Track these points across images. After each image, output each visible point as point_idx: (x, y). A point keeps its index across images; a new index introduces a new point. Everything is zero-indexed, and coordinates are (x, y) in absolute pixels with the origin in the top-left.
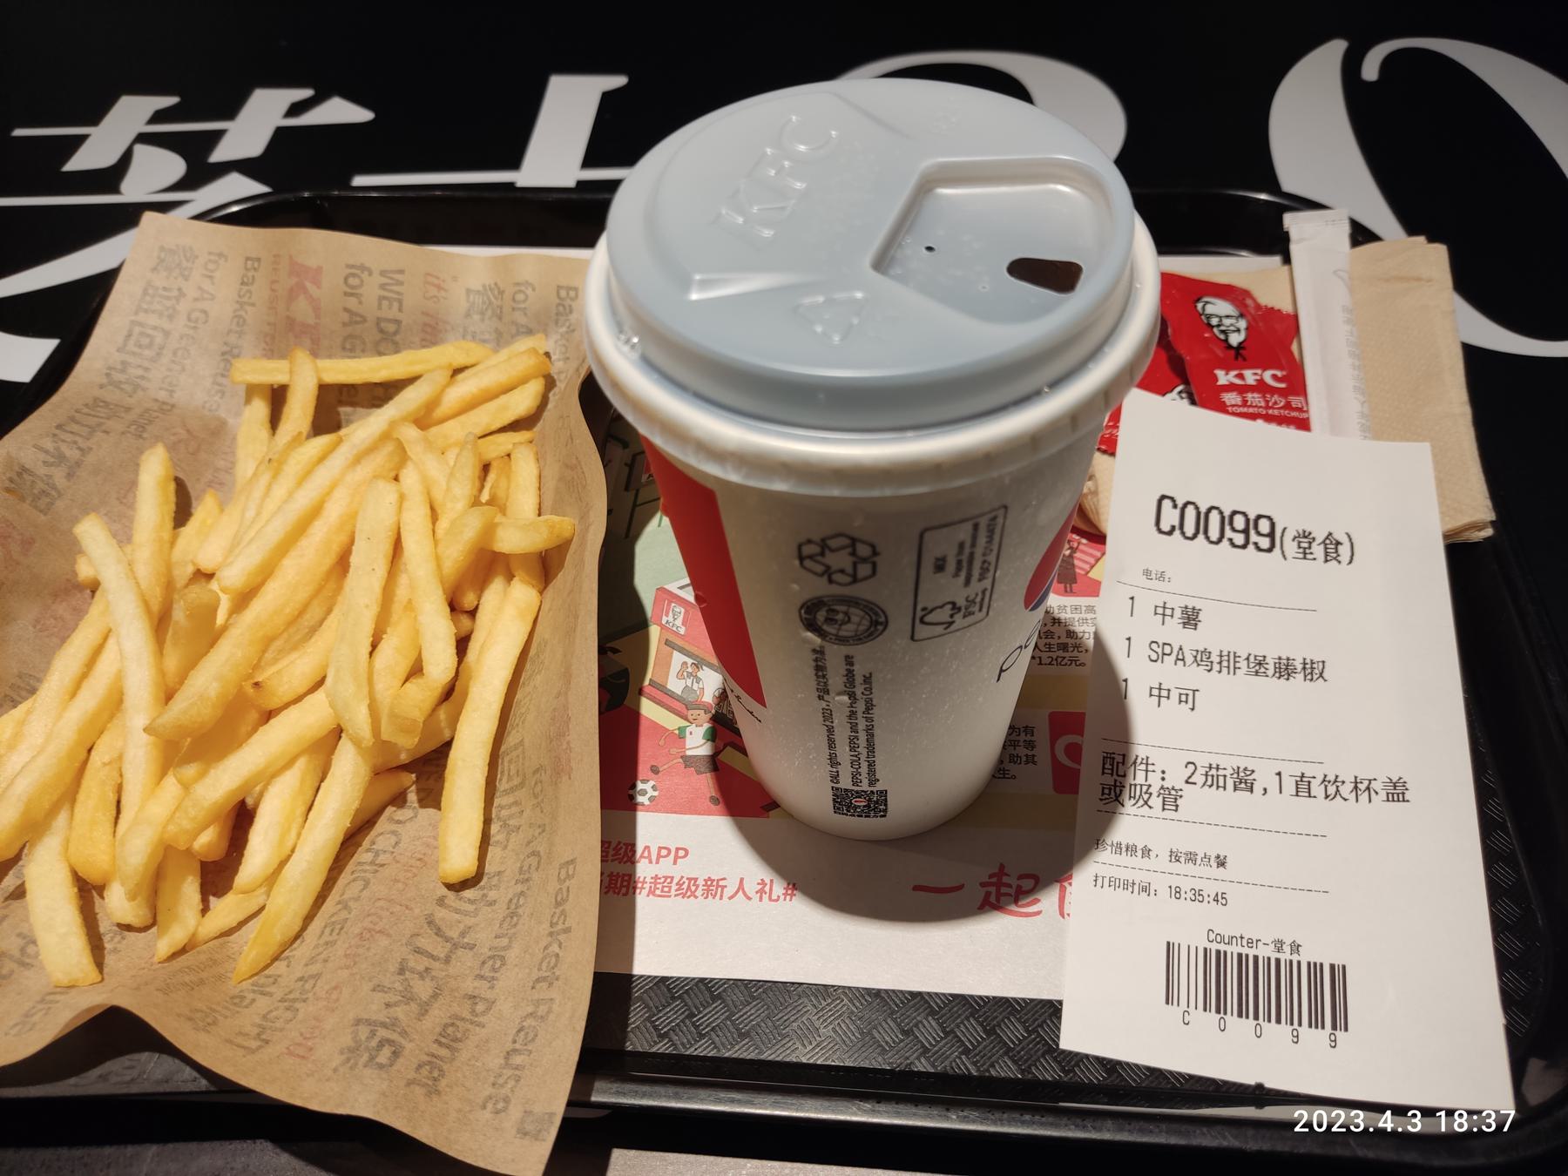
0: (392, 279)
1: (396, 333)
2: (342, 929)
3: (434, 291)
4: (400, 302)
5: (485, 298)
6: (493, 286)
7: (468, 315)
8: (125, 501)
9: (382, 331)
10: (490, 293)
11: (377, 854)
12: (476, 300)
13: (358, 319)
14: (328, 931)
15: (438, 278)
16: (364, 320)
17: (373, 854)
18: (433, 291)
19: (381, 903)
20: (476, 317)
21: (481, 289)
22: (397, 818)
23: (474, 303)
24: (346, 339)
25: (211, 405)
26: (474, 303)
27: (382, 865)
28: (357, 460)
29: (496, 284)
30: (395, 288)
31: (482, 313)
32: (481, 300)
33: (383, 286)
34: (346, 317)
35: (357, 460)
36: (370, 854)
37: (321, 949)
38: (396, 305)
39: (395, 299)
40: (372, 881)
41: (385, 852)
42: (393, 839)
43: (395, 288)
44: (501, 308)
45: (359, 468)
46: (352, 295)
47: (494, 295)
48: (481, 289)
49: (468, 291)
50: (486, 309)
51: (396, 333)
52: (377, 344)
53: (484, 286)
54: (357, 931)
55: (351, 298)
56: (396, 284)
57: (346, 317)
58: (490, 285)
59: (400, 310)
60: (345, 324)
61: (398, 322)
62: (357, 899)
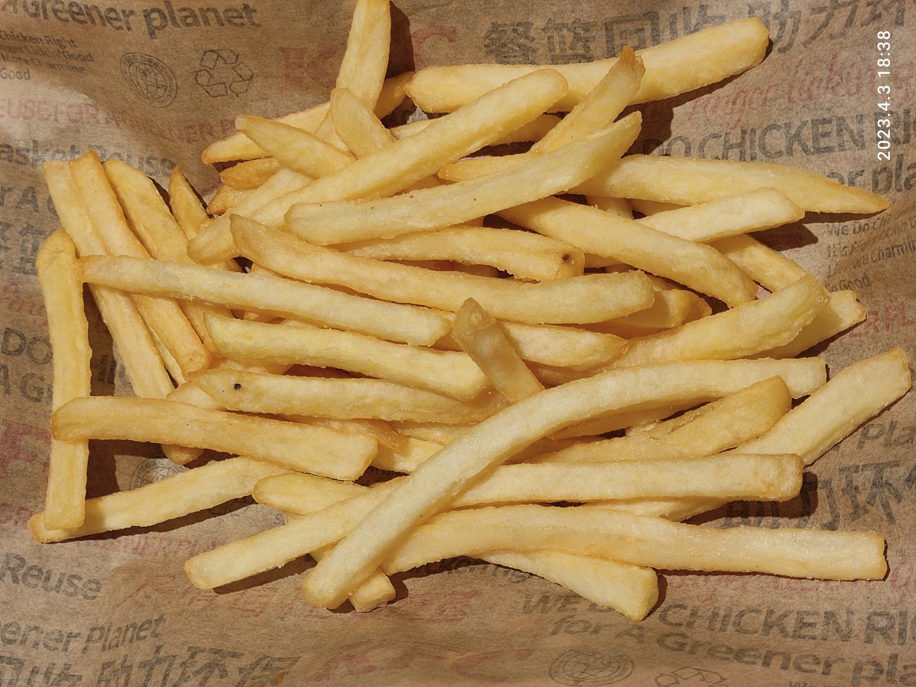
2: (825, 121)
14: (823, 143)
19: (795, 94)
25: (91, 589)
27: (744, 132)
37: (846, 136)
40: (765, 125)
41: (725, 142)
42: (711, 142)
54: (829, 96)
62: (788, 126)
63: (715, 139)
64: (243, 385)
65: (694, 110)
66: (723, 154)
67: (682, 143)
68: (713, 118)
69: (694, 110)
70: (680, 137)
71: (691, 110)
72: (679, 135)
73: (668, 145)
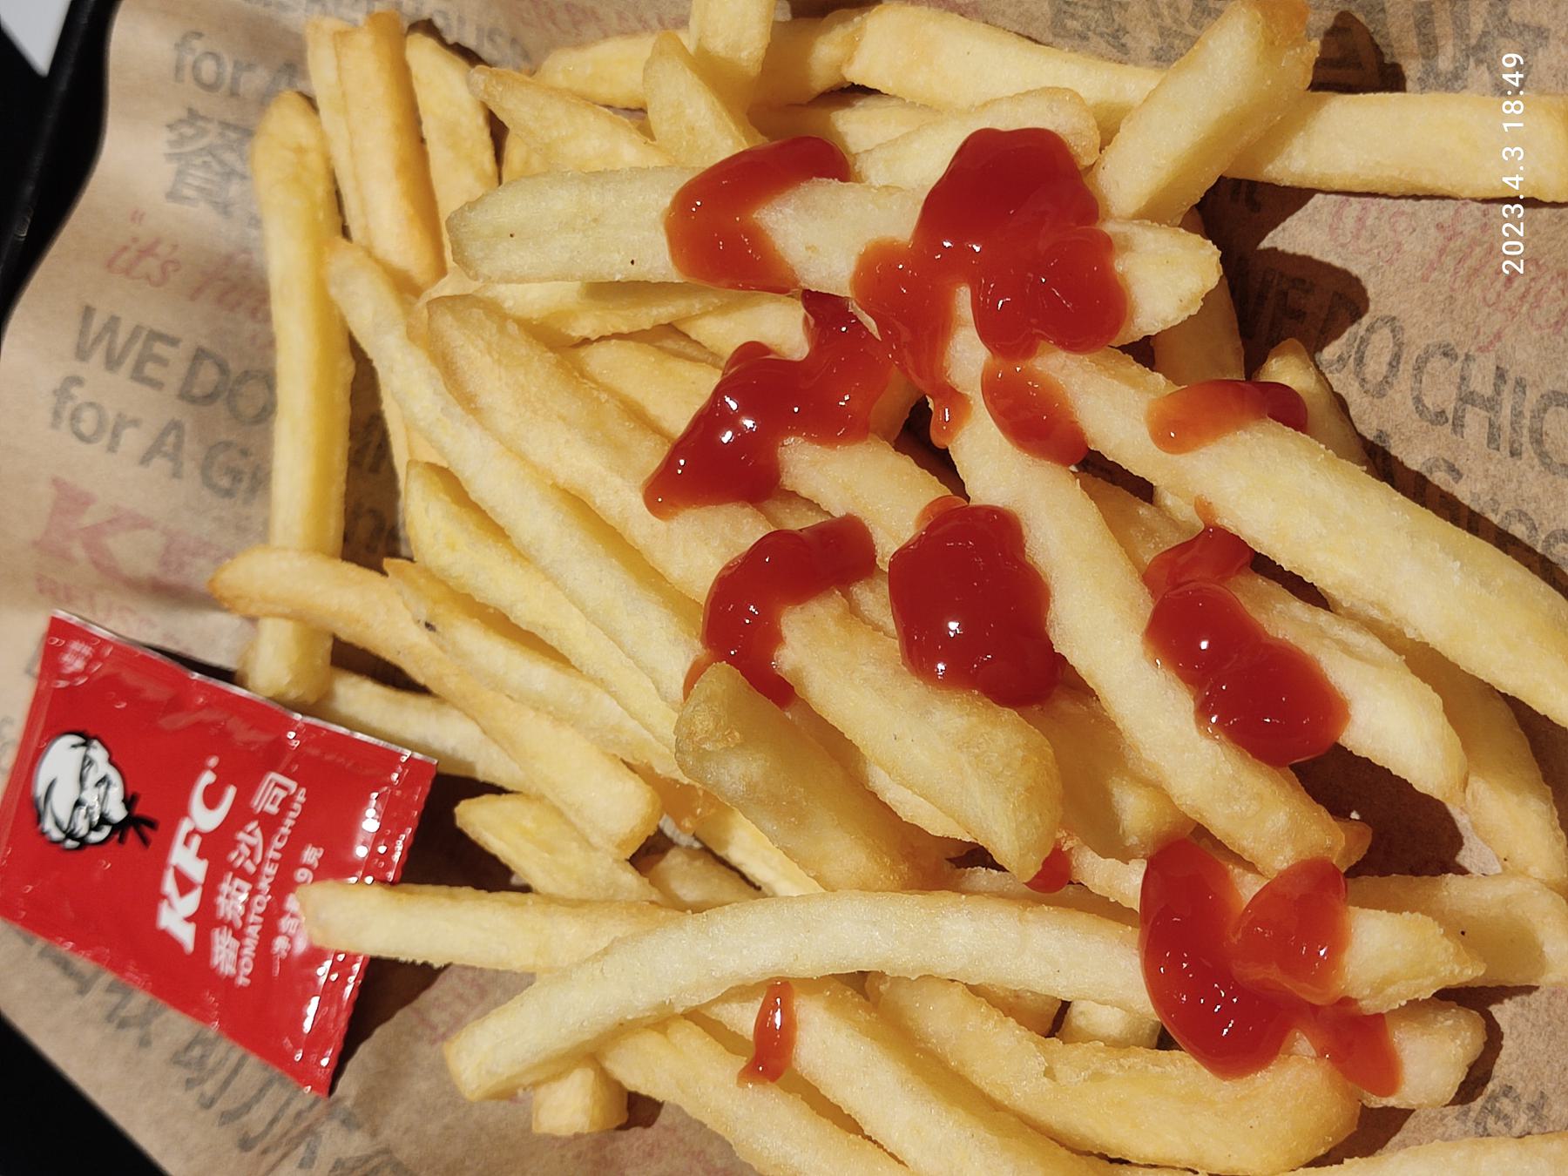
0: (98, 339)
1: (223, 369)
3: (151, 265)
4: (156, 336)
5: (198, 161)
6: (173, 136)
7: (225, 209)
8: (442, 1030)
9: (210, 398)
10: (188, 148)
11: (1467, 399)
12: (196, 183)
13: (171, 439)
15: (125, 248)
16: (176, 426)
17: (1469, 406)
18: (151, 265)
20: (234, 189)
21: (174, 166)
22: (1384, 368)
23: (200, 189)
24: (208, 483)
26: (200, 189)
28: (467, 401)
29: (170, 127)
30: (122, 338)
31: (229, 174)
32: (200, 173)
33: (112, 363)
34: (160, 464)
35: (467, 401)
36: (1468, 418)
38: (160, 348)
39: (146, 345)
41: (1463, 378)
42: (1437, 363)
43: (122, 338)
44: (225, 125)
45: (485, 400)
46: (116, 435)
47: (192, 138)
48: (174, 166)
49: (172, 195)
50: (221, 162)
51: (223, 369)
52: (236, 414)
53: (170, 157)
55: (122, 441)
56: (114, 332)
57: (160, 464)
58: (171, 143)
59: (173, 342)
60: (176, 474)
61: (200, 355)
63: (1445, 360)
64: (439, 628)
65: (1440, 256)
66: (1456, 410)
67: (1390, 335)
68: (1461, 298)
69: (1440, 256)
70: (1394, 318)
71: (1433, 255)
72: (1394, 314)
73: (1368, 330)
